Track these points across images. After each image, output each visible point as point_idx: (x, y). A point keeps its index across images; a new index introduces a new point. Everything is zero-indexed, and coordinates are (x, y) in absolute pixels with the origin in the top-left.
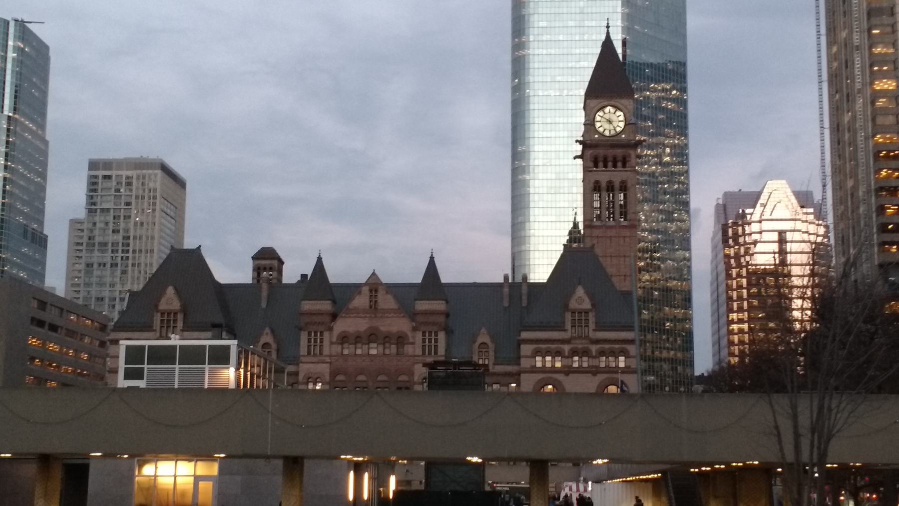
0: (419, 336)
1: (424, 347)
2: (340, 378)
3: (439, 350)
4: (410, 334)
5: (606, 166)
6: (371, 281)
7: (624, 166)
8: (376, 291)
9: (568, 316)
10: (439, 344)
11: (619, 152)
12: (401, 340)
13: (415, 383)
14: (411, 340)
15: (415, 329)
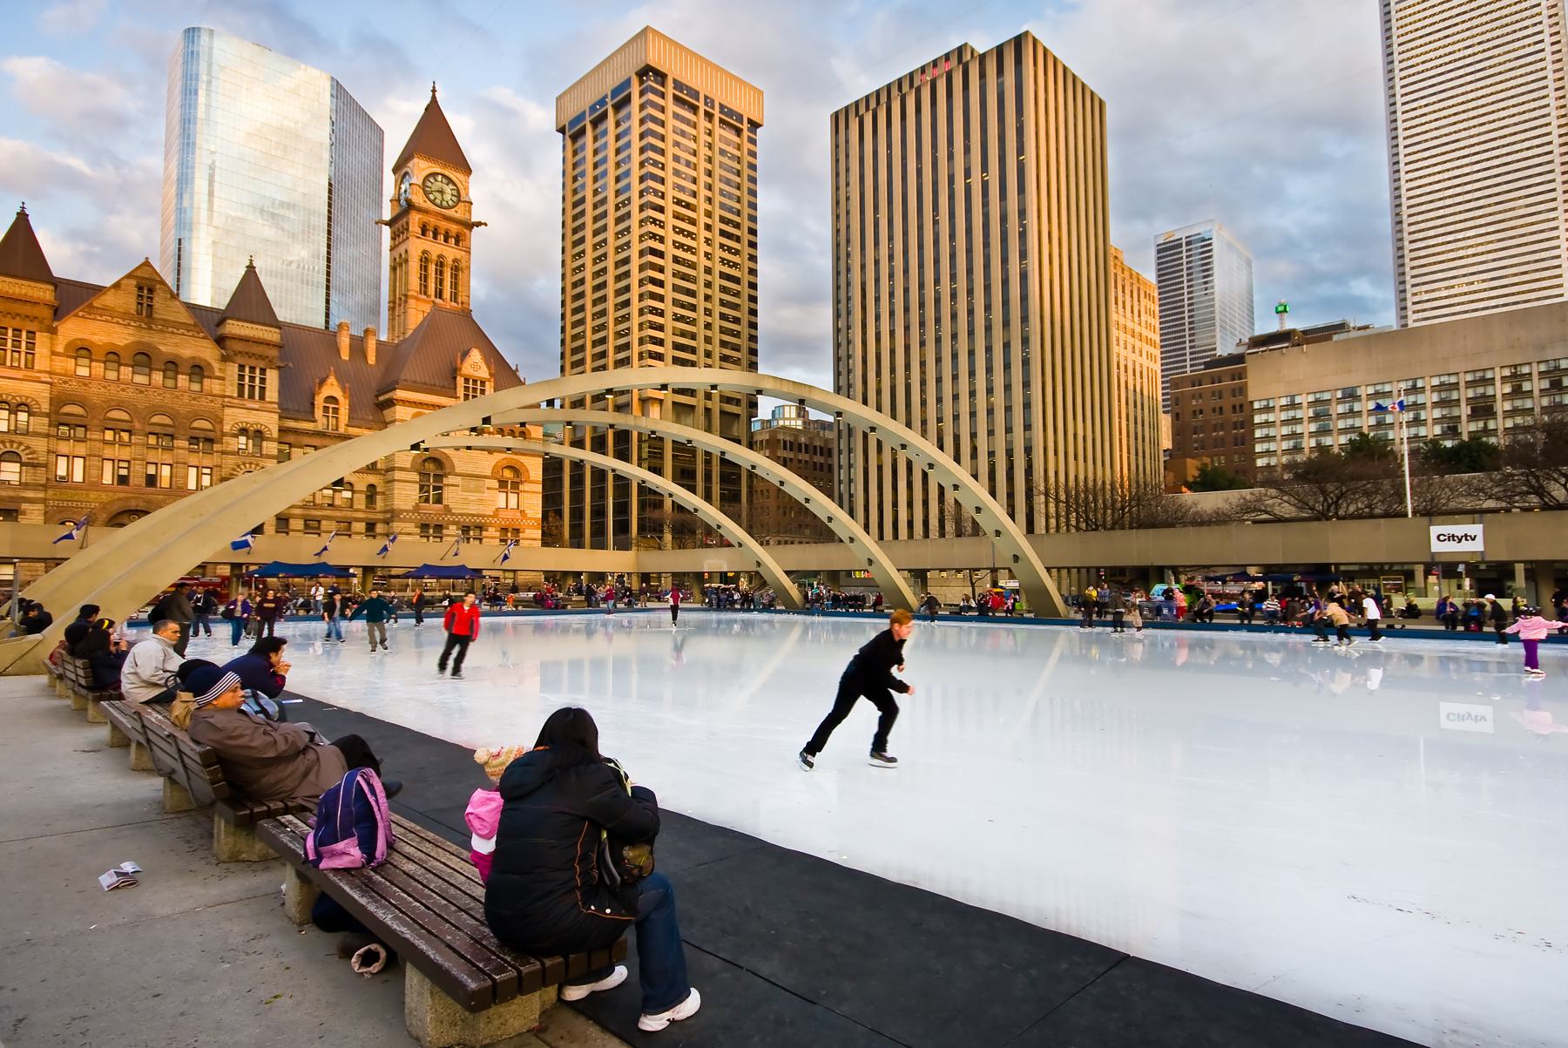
0: (232, 370)
1: (241, 387)
2: (67, 409)
3: (268, 394)
4: (216, 365)
5: (435, 237)
6: (139, 274)
7: (457, 243)
8: (151, 291)
9: (460, 381)
10: (268, 386)
11: (454, 228)
12: (198, 370)
13: (224, 434)
14: (217, 373)
15: (225, 359)
